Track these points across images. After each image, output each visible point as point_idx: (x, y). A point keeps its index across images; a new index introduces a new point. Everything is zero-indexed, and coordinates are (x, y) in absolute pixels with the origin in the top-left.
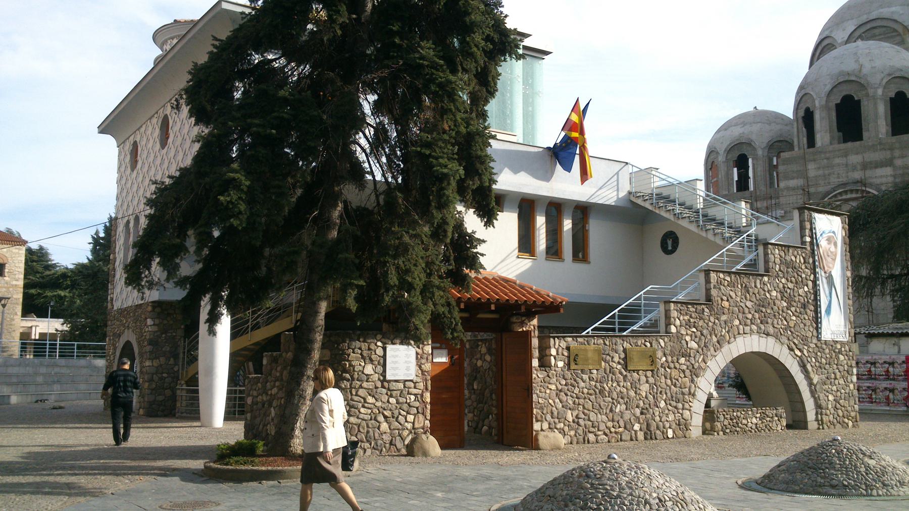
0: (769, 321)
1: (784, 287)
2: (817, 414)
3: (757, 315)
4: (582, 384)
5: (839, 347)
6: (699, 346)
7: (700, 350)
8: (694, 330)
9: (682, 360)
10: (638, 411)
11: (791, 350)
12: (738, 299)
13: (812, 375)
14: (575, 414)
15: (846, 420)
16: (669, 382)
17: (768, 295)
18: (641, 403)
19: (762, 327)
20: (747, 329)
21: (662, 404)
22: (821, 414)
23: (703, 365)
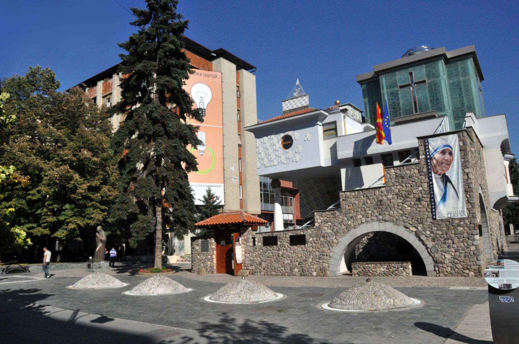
0: (386, 213)
1: (399, 191)
2: (434, 267)
3: (375, 211)
4: (269, 252)
5: (457, 222)
6: (333, 232)
7: (333, 234)
8: (330, 224)
9: (322, 239)
10: (297, 263)
11: (407, 228)
12: (361, 204)
13: (427, 243)
14: (266, 263)
15: (467, 271)
16: (314, 250)
17: (384, 198)
18: (299, 260)
19: (381, 217)
20: (369, 219)
21: (310, 260)
22: (438, 267)
23: (335, 241)
